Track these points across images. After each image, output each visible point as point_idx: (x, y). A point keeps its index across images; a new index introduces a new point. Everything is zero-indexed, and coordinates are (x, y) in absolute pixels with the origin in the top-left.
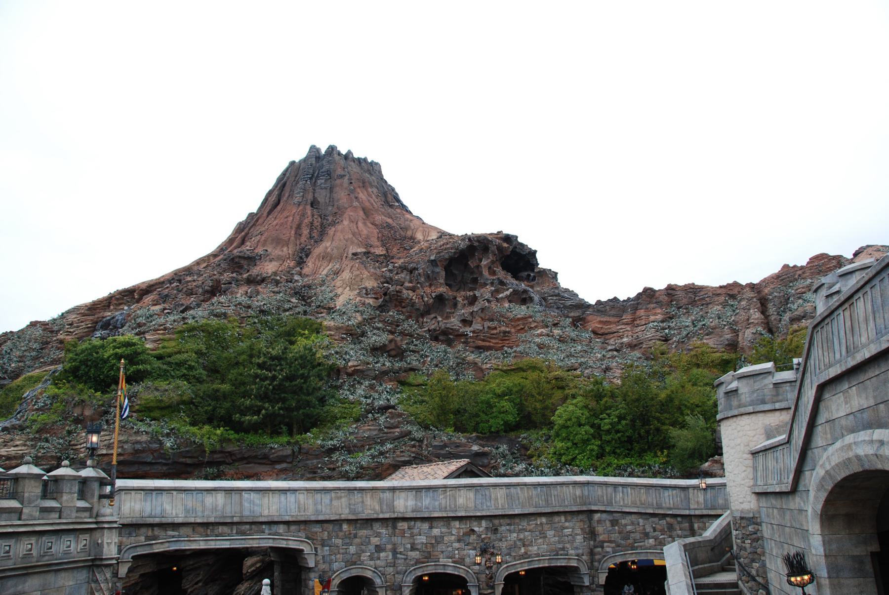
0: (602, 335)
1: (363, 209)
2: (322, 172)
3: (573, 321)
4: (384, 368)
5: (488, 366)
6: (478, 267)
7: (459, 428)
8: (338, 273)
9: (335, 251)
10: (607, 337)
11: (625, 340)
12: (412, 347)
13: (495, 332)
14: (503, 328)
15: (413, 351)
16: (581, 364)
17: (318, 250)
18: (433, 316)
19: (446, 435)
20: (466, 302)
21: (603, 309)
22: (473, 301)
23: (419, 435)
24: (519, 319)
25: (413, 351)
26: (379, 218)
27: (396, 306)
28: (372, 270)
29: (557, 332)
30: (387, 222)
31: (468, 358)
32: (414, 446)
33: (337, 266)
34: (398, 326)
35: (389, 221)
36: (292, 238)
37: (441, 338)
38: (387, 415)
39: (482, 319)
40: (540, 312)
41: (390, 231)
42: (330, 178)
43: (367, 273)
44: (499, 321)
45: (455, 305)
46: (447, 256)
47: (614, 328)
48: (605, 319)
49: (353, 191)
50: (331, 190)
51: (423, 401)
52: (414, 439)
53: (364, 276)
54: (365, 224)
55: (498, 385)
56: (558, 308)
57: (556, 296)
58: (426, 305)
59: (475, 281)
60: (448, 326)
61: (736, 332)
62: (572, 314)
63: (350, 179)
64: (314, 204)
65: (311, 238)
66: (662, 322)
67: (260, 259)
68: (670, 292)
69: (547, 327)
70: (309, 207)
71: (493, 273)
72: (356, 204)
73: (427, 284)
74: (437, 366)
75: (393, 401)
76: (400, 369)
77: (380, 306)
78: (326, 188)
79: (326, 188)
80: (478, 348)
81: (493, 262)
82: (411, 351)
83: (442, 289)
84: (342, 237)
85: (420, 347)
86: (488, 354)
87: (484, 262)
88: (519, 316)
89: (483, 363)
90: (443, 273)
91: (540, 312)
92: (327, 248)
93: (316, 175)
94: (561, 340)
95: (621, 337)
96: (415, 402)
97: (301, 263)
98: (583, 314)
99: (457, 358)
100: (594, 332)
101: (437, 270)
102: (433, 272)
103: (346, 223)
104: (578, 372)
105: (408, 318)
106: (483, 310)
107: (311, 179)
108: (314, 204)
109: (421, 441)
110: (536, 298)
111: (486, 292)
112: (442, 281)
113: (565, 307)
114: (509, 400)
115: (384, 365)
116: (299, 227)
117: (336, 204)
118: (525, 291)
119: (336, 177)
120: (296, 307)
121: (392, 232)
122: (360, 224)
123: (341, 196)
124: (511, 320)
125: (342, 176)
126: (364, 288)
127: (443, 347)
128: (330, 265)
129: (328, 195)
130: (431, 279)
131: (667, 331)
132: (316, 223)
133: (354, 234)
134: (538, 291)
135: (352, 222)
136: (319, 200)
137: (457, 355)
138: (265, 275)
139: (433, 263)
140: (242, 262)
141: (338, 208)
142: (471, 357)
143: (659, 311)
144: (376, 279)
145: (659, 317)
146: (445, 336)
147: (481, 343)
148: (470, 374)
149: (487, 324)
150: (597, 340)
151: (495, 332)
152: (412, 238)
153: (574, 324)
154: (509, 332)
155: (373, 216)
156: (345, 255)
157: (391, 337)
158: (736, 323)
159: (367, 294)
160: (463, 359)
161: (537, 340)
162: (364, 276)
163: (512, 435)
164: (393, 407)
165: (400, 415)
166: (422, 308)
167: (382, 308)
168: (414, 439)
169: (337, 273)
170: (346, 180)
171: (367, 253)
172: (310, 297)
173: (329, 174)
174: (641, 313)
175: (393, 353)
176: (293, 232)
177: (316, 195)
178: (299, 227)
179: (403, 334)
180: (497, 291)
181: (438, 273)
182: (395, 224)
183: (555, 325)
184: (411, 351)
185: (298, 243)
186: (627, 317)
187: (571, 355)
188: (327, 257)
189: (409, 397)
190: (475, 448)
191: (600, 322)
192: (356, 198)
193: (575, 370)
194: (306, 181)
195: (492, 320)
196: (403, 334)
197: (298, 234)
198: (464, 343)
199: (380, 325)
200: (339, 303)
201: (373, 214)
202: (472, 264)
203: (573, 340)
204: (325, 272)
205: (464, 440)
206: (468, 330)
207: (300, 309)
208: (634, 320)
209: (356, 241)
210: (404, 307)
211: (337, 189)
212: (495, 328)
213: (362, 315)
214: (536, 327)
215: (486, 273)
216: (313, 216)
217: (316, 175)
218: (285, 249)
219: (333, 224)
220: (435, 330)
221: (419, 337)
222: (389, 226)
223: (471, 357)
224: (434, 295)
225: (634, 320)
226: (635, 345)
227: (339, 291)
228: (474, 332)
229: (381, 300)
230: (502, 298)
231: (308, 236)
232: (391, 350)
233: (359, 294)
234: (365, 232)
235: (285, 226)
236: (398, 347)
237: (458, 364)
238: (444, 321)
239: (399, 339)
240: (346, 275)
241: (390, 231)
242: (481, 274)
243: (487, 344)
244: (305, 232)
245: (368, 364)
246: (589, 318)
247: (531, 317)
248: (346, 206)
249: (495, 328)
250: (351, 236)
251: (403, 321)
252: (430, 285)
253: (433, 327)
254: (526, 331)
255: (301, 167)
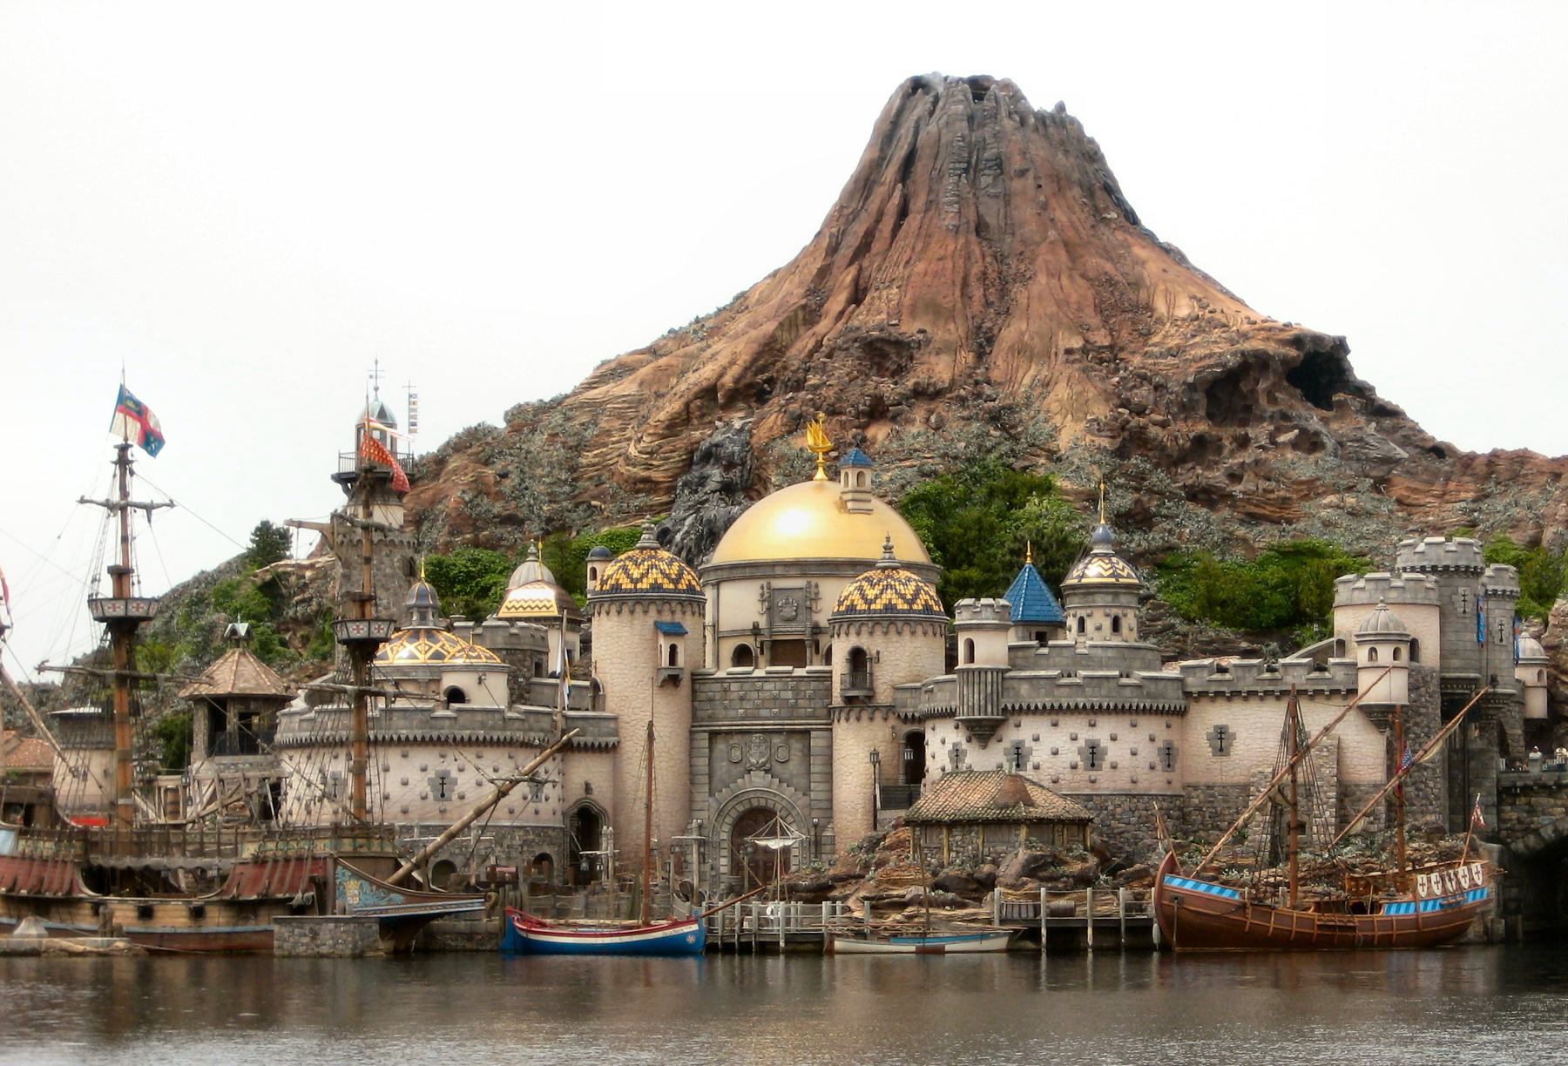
0: (1409, 505)
1: (1066, 245)
2: (987, 160)
3: (1375, 483)
4: (1140, 549)
5: (1261, 545)
6: (1253, 391)
7: (1226, 622)
8: (1048, 385)
9: (1037, 340)
10: (1414, 510)
11: (1431, 518)
12: (1164, 511)
13: (1272, 496)
14: (1282, 493)
15: (1166, 517)
16: (1371, 550)
17: (1008, 335)
18: (1190, 465)
19: (1212, 630)
20: (1234, 445)
21: (1414, 470)
22: (1243, 443)
23: (1183, 628)
24: (1302, 483)
25: (1166, 517)
26: (1094, 262)
27: (1139, 447)
28: (1099, 384)
29: (1350, 500)
30: (1106, 273)
31: (1237, 533)
32: (1178, 641)
33: (1045, 372)
34: (1144, 479)
35: (1108, 267)
36: (959, 305)
37: (1201, 496)
38: (1148, 606)
39: (1256, 475)
40: (1332, 469)
41: (1112, 293)
42: (1002, 173)
43: (1092, 389)
44: (1278, 481)
45: (1219, 450)
46: (1210, 377)
47: (1423, 500)
48: (1414, 485)
49: (1045, 207)
50: (1007, 198)
51: (1184, 588)
52: (1177, 634)
53: (1090, 395)
54: (1071, 277)
55: (1272, 574)
56: (1358, 460)
57: (1357, 441)
58: (1181, 449)
59: (1248, 409)
60: (1211, 482)
61: (1540, 528)
62: (1374, 473)
63: (1036, 178)
64: (980, 228)
65: (988, 304)
66: (1474, 501)
67: (919, 348)
68: (1494, 459)
69: (1338, 492)
70: (973, 237)
71: (1273, 400)
72: (1052, 234)
73: (1182, 416)
74: (1198, 541)
75: (1153, 590)
76: (1158, 548)
77: (1118, 449)
78: (996, 196)
79: (996, 196)
80: (1252, 516)
81: (1274, 385)
82: (1162, 516)
83: (1202, 427)
84: (1041, 311)
85: (1174, 510)
86: (1261, 528)
87: (1262, 386)
88: (1303, 478)
89: (1254, 541)
90: (1204, 402)
91: (1332, 469)
92: (1023, 334)
93: (973, 161)
94: (1353, 514)
95: (1426, 514)
96: (1175, 590)
97: (981, 355)
98: (1389, 472)
99: (1223, 531)
100: (1399, 502)
101: (1196, 396)
102: (1190, 400)
103: (1042, 279)
104: (1367, 559)
105: (1157, 466)
106: (1257, 462)
107: (966, 171)
108: (980, 228)
109: (1185, 635)
110: (1330, 443)
111: (1259, 432)
112: (1202, 413)
113: (1368, 459)
114: (1283, 593)
115: (1139, 545)
116: (965, 284)
117: (1018, 233)
118: (1317, 434)
119: (1012, 173)
120: (999, 444)
121: (1116, 293)
122: (1065, 281)
123: (1025, 213)
124: (1294, 483)
125: (1022, 173)
126: (1094, 420)
127: (1203, 511)
128: (1033, 367)
129: (1002, 211)
130: (1186, 409)
131: (1476, 514)
132: (992, 275)
133: (1058, 304)
134: (1336, 431)
135: (1053, 275)
136: (988, 219)
137: (1223, 527)
138: (940, 386)
139: (1192, 387)
140: (887, 348)
141: (1023, 242)
142: (1241, 531)
143: (1471, 486)
144: (1107, 400)
145: (1471, 495)
146: (1205, 496)
147: (1252, 509)
148: (1239, 554)
149: (1264, 484)
150: (1400, 514)
151: (1272, 496)
152: (1149, 308)
153: (1376, 488)
154: (1289, 499)
155: (1083, 260)
156: (1053, 350)
157: (1136, 495)
158: (1543, 516)
159: (1099, 430)
160: (1231, 533)
161: (1323, 513)
162: (1090, 395)
163: (1284, 631)
164: (1153, 597)
165: (1161, 606)
166: (1175, 454)
167: (1121, 453)
168: (1177, 634)
169: (1046, 385)
170: (1030, 181)
171: (1084, 351)
172: (1014, 427)
173: (999, 164)
174: (1452, 485)
175: (1139, 518)
176: (958, 293)
177: (982, 210)
178: (965, 284)
179: (1150, 491)
180: (1279, 430)
181: (1197, 401)
182: (1119, 278)
183: (1350, 489)
184: (1162, 516)
185: (969, 315)
186: (1437, 489)
187: (1362, 537)
188: (1022, 350)
189: (1168, 585)
190: (1244, 645)
191: (1408, 488)
192: (1052, 220)
193: (1364, 555)
194: (960, 176)
195: (1269, 479)
196: (1150, 491)
197: (965, 294)
198: (1230, 506)
199: (1122, 481)
200: (1063, 442)
201: (1082, 256)
202: (1244, 387)
203: (1369, 514)
204: (1027, 381)
205: (1232, 636)
206: (1237, 489)
207: (1004, 448)
208: (1444, 494)
209: (1065, 320)
210: (1150, 450)
211: (1017, 201)
212: (1272, 491)
213: (1100, 468)
214: (1324, 493)
215: (1263, 401)
216: (984, 257)
217: (973, 161)
218: (952, 327)
219: (1025, 279)
220: (1192, 486)
221: (1172, 496)
222: (1111, 282)
223: (1241, 531)
224: (1192, 435)
225: (1444, 494)
226: (1439, 529)
227: (1058, 420)
228: (1244, 493)
229: (1120, 439)
230: (1284, 443)
231: (983, 301)
232: (1137, 514)
233: (1089, 431)
234: (1074, 298)
235: (943, 279)
236: (1147, 511)
237: (1224, 540)
238: (1206, 473)
239: (1145, 499)
240: (1061, 391)
241: (1112, 293)
242: (1257, 401)
243: (1262, 511)
244: (977, 293)
245: (1122, 544)
246: (1396, 480)
247: (1318, 479)
248: (1037, 238)
249: (1272, 491)
250: (1055, 309)
251: (1150, 471)
252: (1185, 420)
253: (1190, 482)
254: (1312, 499)
255: (943, 140)
